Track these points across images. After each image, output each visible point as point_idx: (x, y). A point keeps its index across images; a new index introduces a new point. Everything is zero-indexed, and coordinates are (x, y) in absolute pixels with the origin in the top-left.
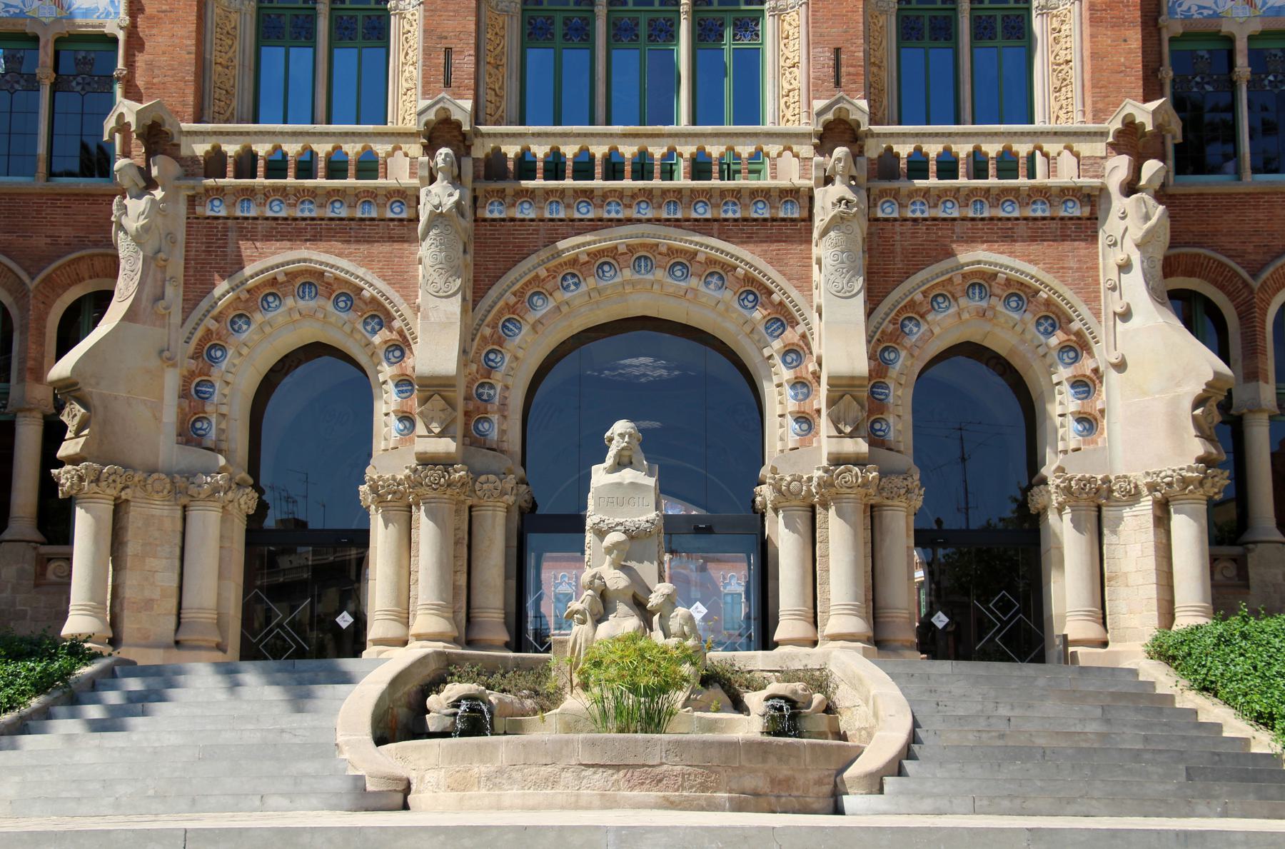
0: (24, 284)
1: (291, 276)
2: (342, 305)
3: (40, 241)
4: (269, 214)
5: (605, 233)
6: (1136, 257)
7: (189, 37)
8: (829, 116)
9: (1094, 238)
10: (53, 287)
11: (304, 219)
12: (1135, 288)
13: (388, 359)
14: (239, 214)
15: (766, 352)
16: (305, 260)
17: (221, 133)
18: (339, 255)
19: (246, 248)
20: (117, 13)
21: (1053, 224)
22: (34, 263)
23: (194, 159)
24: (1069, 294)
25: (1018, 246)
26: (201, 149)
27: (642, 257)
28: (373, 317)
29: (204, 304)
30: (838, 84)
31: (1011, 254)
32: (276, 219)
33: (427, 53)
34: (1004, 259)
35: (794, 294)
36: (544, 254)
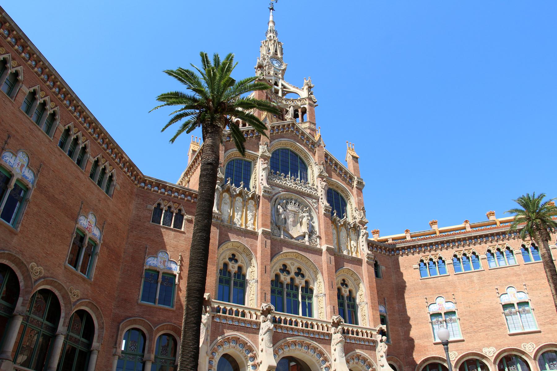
0: (152, 329)
1: (232, 338)
2: (241, 346)
3: (156, 319)
4: (229, 323)
5: (295, 337)
6: (384, 355)
7: (214, 281)
8: (338, 320)
9: (375, 350)
10: (158, 331)
11: (235, 325)
12: (384, 361)
13: (250, 360)
14: (222, 322)
15: (322, 367)
16: (236, 335)
17: (220, 303)
18: (243, 335)
19: (225, 331)
20: (177, 270)
21: (369, 346)
22: (156, 324)
23: (214, 308)
24: (373, 361)
25: (364, 350)
26: (216, 306)
27: (302, 344)
28: (247, 350)
29: (215, 342)
30: (334, 313)
31: (363, 351)
32: (230, 324)
33: (261, 293)
34: (362, 352)
35: (329, 355)
36: (283, 340)
